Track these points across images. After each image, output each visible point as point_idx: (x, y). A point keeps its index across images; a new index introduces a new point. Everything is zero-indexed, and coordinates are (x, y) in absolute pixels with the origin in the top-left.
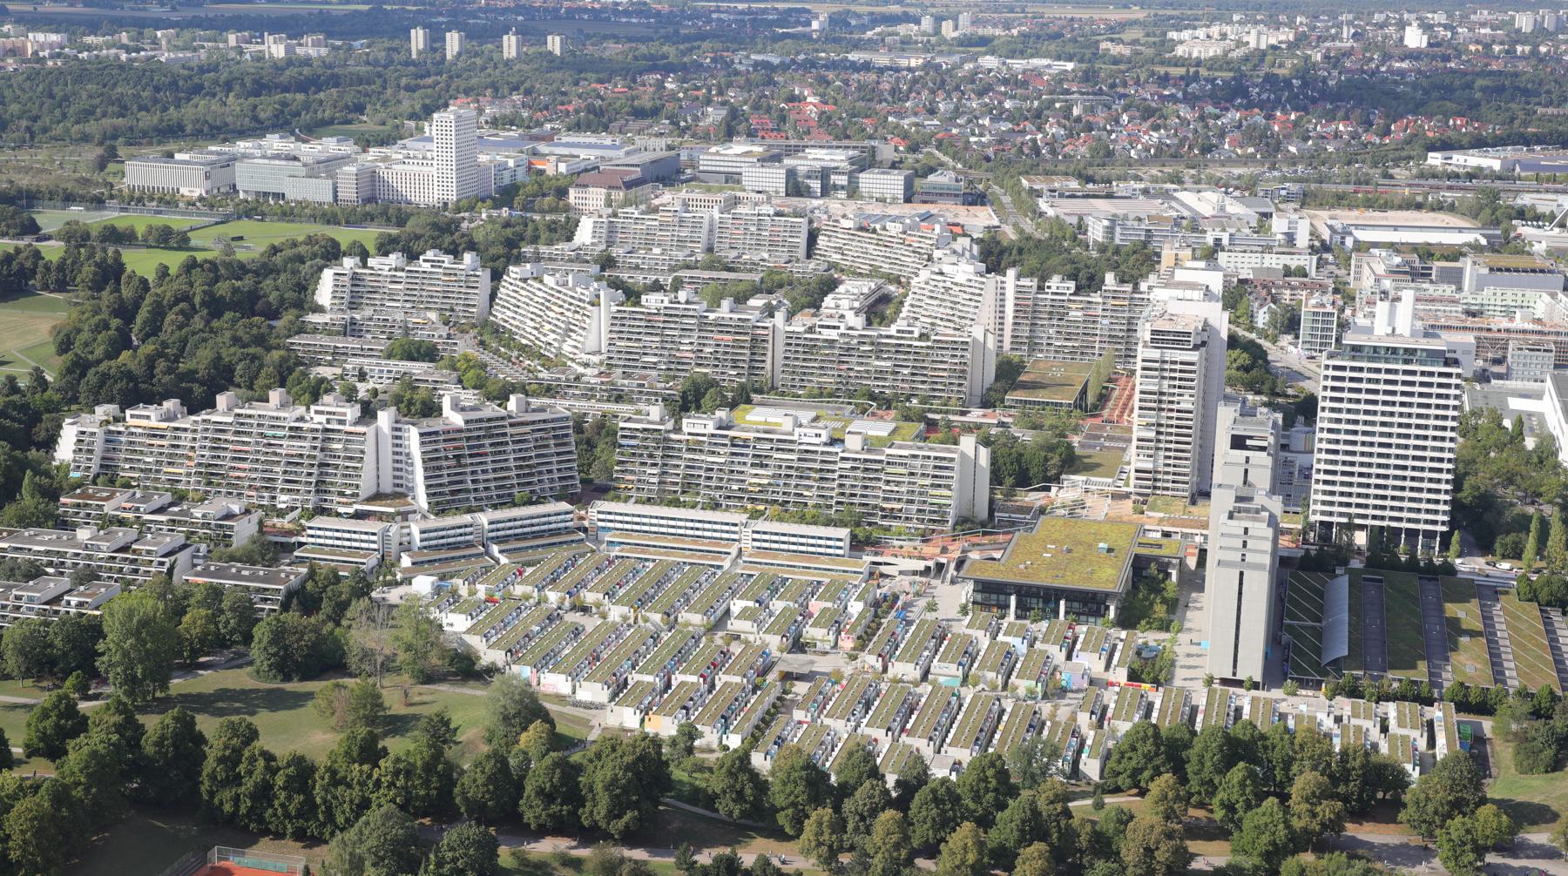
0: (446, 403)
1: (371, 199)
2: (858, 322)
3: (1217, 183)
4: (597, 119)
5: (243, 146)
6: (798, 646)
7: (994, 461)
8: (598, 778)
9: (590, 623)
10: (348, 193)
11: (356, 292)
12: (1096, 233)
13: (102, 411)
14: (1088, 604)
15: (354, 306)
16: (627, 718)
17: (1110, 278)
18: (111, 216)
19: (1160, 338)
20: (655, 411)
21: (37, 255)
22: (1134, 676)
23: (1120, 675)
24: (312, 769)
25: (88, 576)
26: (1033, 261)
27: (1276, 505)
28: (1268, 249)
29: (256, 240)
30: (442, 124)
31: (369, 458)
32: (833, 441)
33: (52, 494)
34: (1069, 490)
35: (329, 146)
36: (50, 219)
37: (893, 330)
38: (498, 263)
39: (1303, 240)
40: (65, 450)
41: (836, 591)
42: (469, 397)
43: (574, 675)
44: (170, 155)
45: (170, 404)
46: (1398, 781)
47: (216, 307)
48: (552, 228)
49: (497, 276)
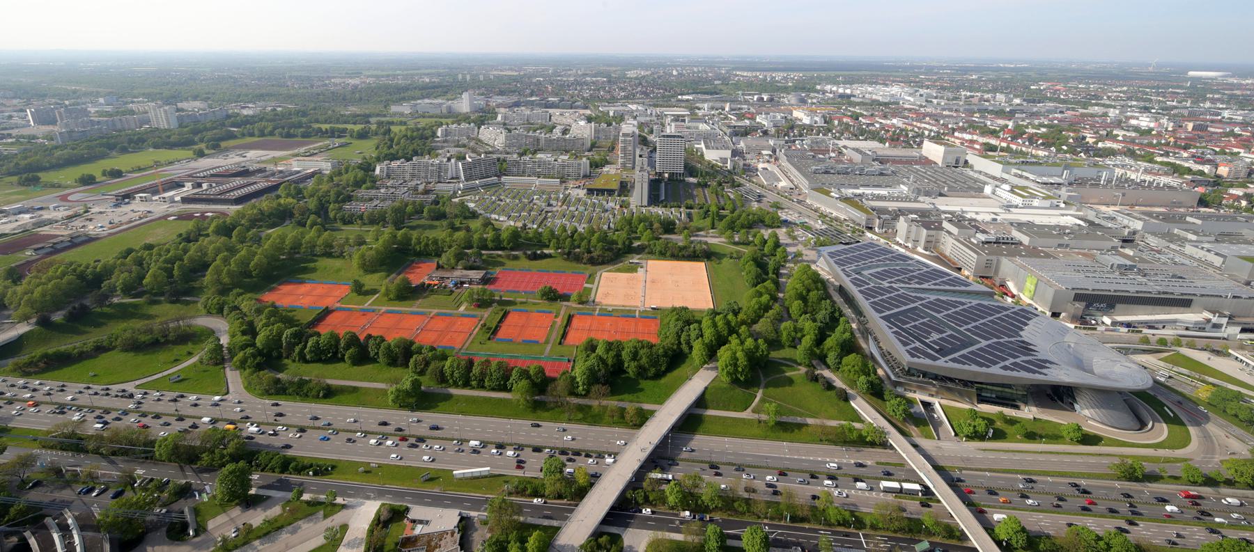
0: (467, 156)
1: (450, 112)
2: (560, 134)
3: (635, 103)
4: (501, 93)
5: (419, 101)
6: (549, 205)
7: (590, 163)
8: (504, 236)
9: (502, 203)
10: (444, 111)
11: (447, 133)
12: (611, 114)
13: (386, 162)
14: (611, 192)
15: (446, 136)
16: (512, 223)
17: (614, 123)
18: (388, 119)
19: (624, 135)
20: (515, 156)
21: (370, 128)
22: (621, 206)
23: (618, 207)
24: (438, 240)
25: (384, 200)
26: (597, 120)
27: (649, 169)
28: (647, 116)
29: (423, 123)
30: (465, 96)
31: (450, 170)
32: (555, 161)
33: (374, 182)
34: (605, 169)
35: (439, 101)
36: (373, 120)
37: (568, 136)
38: (480, 123)
39: (654, 114)
40: (377, 171)
41: (557, 192)
42: (473, 155)
43: (499, 214)
44: (402, 105)
45: (402, 160)
46: (674, 224)
47: (413, 138)
48: (492, 117)
49: (479, 128)
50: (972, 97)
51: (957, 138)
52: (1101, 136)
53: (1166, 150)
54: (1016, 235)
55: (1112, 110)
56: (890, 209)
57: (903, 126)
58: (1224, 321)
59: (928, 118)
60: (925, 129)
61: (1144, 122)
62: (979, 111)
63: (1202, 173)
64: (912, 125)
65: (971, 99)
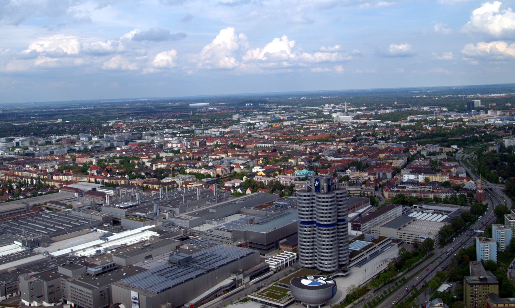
50: (61, 139)
51: (56, 181)
52: (154, 159)
53: (192, 162)
54: (117, 260)
55: (155, 137)
56: (9, 271)
57: (7, 178)
58: (241, 276)
59: (27, 166)
60: (26, 177)
61: (175, 145)
62: (69, 151)
63: (209, 176)
64: (14, 175)
65: (60, 142)
